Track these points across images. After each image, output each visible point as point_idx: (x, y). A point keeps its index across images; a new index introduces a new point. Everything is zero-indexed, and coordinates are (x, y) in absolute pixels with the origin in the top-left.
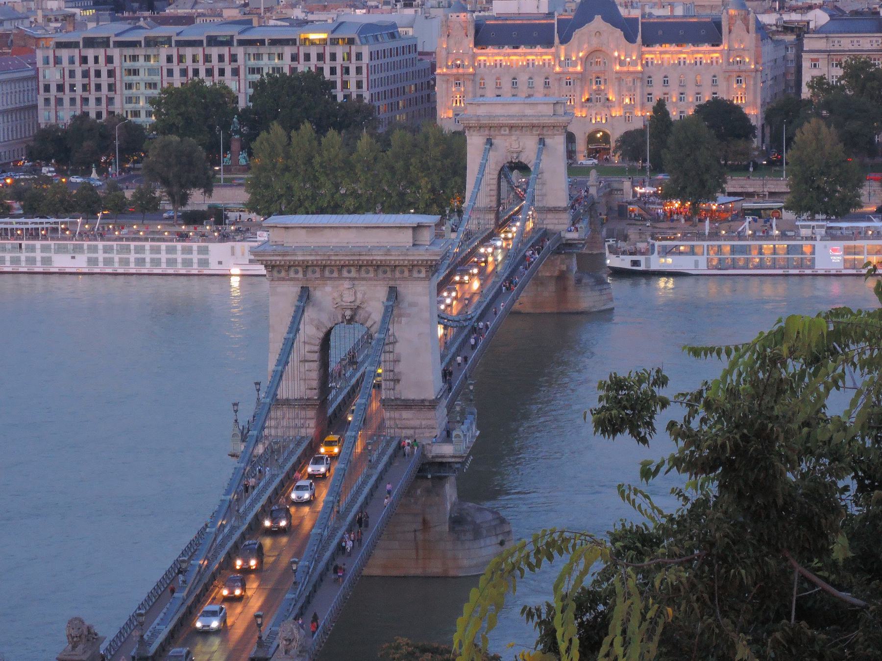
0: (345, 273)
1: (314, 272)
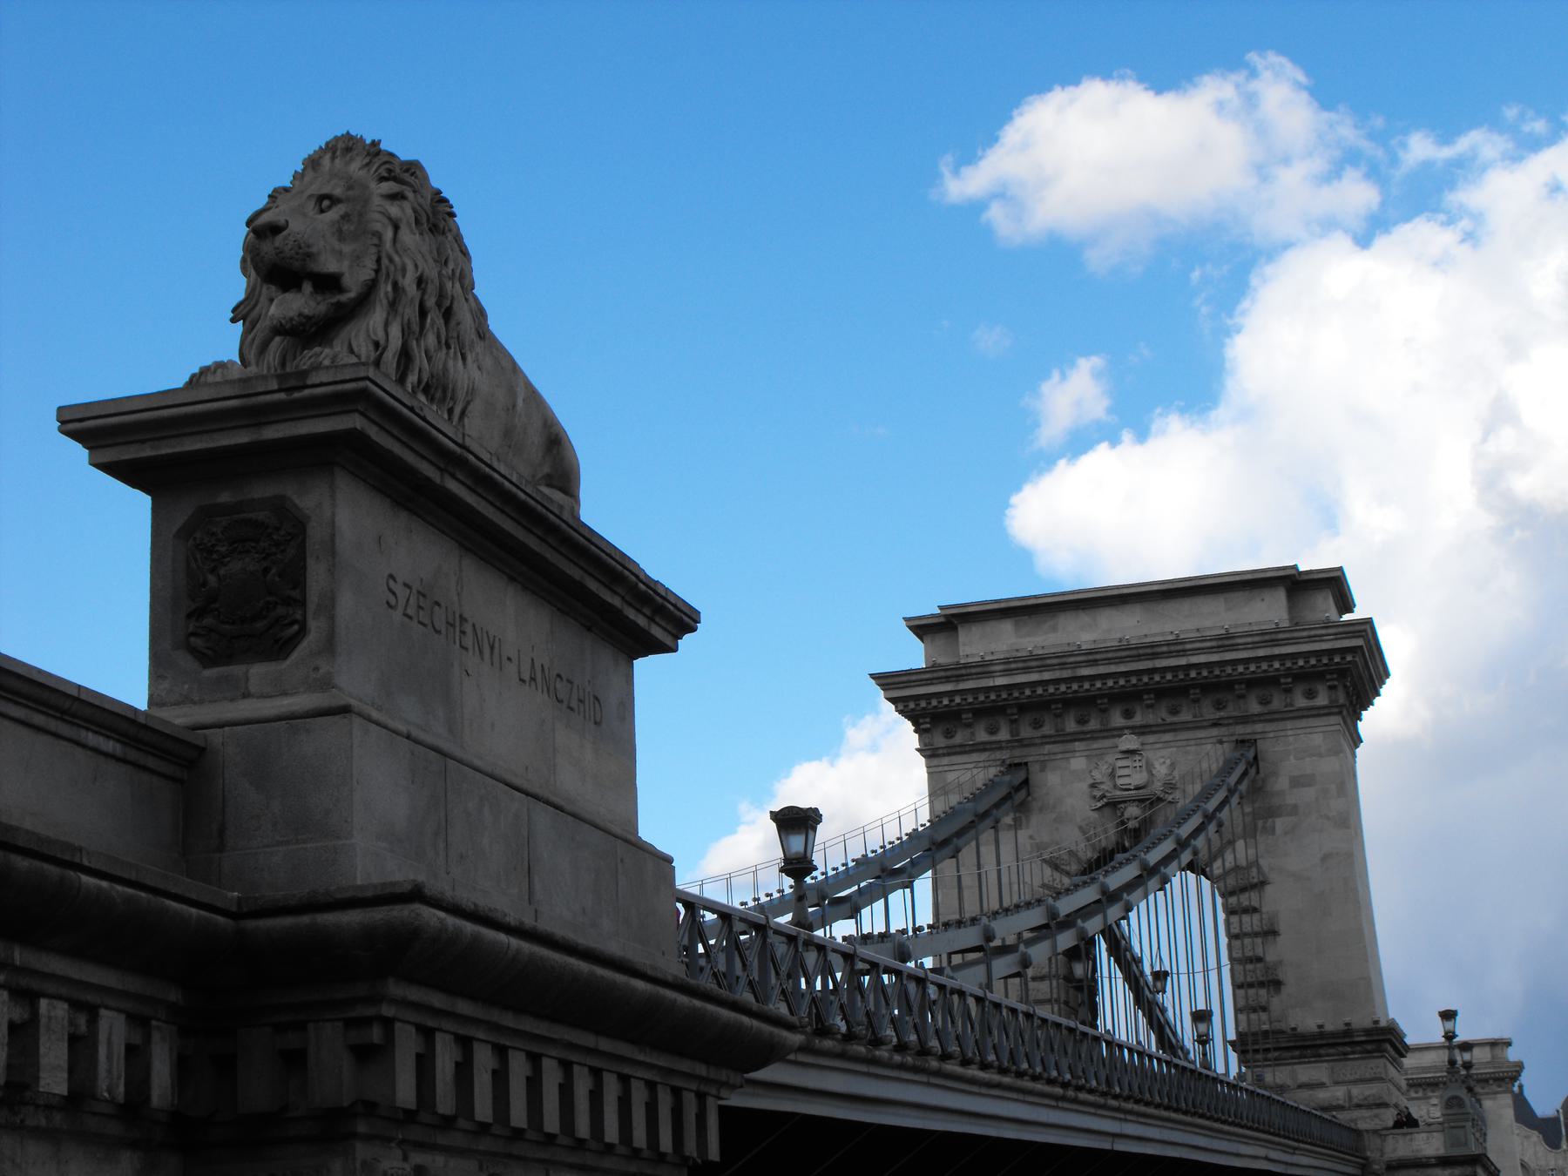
0: (1117, 720)
1: (1037, 725)
